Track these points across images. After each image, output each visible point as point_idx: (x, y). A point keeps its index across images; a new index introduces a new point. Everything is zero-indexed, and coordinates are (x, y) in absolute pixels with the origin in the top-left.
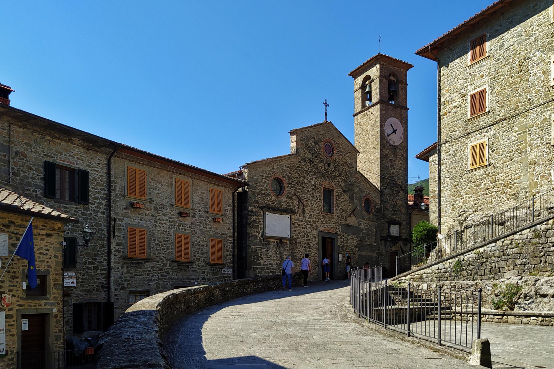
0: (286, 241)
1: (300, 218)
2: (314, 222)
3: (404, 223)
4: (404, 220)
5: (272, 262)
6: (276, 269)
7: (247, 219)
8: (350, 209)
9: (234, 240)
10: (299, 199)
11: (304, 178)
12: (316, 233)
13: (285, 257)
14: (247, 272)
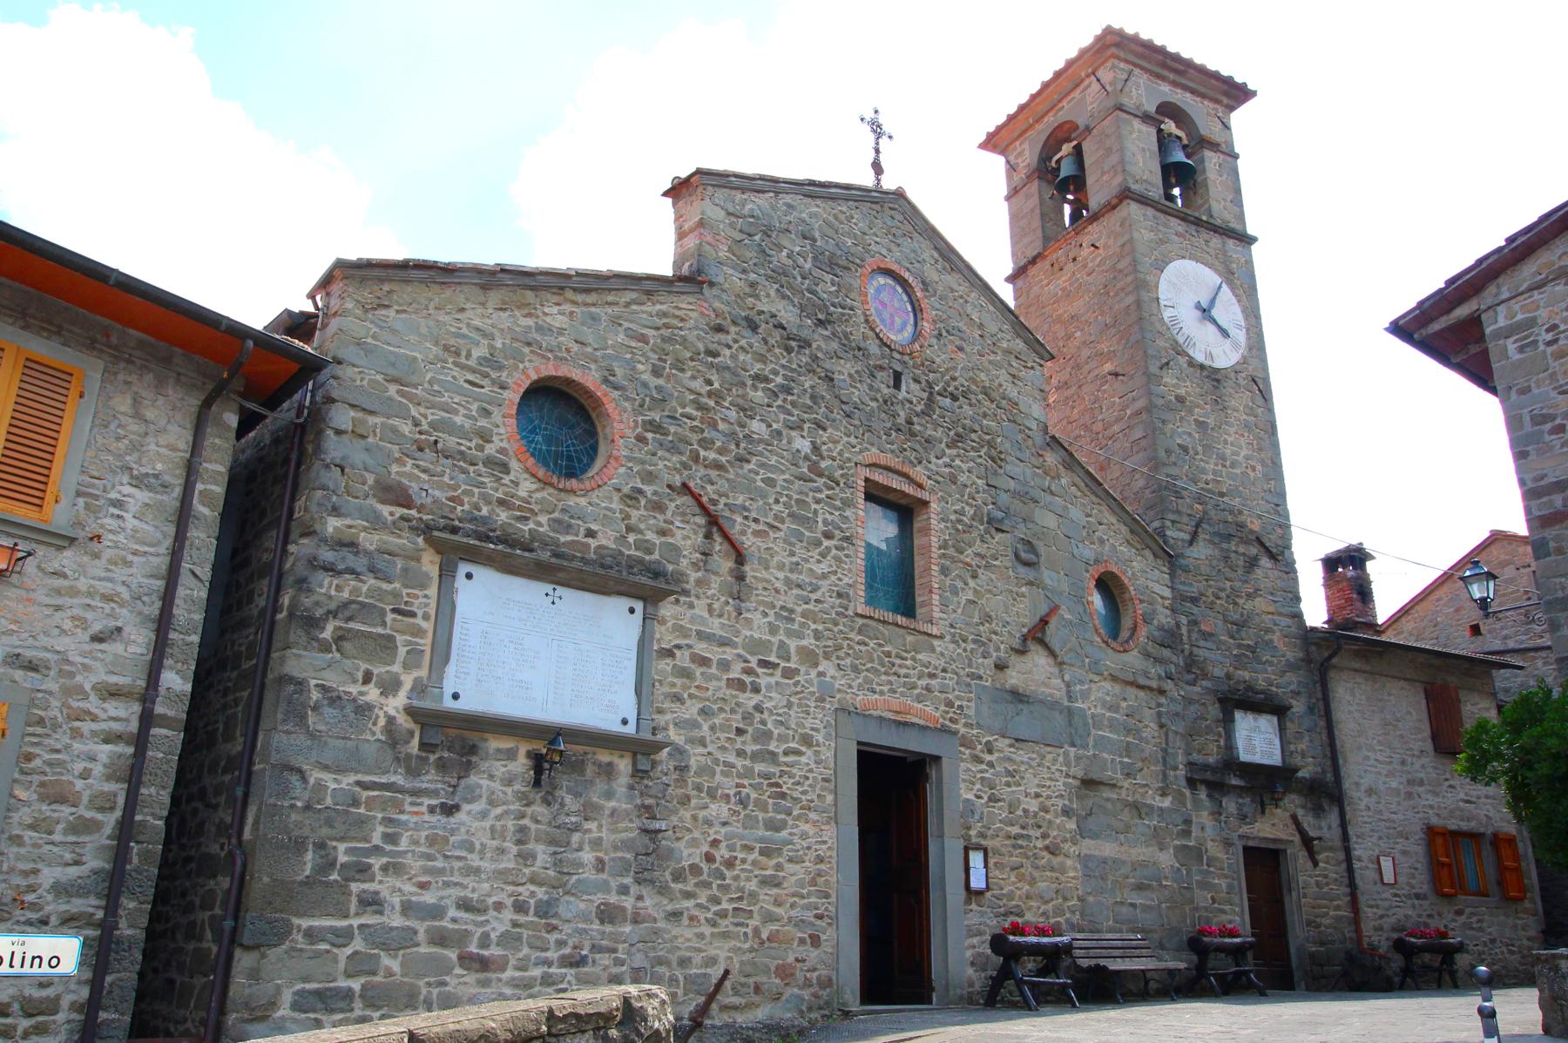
0: (604, 757)
1: (715, 626)
2: (809, 657)
3: (1298, 706)
5: (477, 889)
6: (509, 940)
7: (302, 583)
8: (1024, 613)
9: (147, 719)
10: (714, 523)
11: (747, 411)
12: (817, 721)
13: (587, 856)
14: (243, 961)
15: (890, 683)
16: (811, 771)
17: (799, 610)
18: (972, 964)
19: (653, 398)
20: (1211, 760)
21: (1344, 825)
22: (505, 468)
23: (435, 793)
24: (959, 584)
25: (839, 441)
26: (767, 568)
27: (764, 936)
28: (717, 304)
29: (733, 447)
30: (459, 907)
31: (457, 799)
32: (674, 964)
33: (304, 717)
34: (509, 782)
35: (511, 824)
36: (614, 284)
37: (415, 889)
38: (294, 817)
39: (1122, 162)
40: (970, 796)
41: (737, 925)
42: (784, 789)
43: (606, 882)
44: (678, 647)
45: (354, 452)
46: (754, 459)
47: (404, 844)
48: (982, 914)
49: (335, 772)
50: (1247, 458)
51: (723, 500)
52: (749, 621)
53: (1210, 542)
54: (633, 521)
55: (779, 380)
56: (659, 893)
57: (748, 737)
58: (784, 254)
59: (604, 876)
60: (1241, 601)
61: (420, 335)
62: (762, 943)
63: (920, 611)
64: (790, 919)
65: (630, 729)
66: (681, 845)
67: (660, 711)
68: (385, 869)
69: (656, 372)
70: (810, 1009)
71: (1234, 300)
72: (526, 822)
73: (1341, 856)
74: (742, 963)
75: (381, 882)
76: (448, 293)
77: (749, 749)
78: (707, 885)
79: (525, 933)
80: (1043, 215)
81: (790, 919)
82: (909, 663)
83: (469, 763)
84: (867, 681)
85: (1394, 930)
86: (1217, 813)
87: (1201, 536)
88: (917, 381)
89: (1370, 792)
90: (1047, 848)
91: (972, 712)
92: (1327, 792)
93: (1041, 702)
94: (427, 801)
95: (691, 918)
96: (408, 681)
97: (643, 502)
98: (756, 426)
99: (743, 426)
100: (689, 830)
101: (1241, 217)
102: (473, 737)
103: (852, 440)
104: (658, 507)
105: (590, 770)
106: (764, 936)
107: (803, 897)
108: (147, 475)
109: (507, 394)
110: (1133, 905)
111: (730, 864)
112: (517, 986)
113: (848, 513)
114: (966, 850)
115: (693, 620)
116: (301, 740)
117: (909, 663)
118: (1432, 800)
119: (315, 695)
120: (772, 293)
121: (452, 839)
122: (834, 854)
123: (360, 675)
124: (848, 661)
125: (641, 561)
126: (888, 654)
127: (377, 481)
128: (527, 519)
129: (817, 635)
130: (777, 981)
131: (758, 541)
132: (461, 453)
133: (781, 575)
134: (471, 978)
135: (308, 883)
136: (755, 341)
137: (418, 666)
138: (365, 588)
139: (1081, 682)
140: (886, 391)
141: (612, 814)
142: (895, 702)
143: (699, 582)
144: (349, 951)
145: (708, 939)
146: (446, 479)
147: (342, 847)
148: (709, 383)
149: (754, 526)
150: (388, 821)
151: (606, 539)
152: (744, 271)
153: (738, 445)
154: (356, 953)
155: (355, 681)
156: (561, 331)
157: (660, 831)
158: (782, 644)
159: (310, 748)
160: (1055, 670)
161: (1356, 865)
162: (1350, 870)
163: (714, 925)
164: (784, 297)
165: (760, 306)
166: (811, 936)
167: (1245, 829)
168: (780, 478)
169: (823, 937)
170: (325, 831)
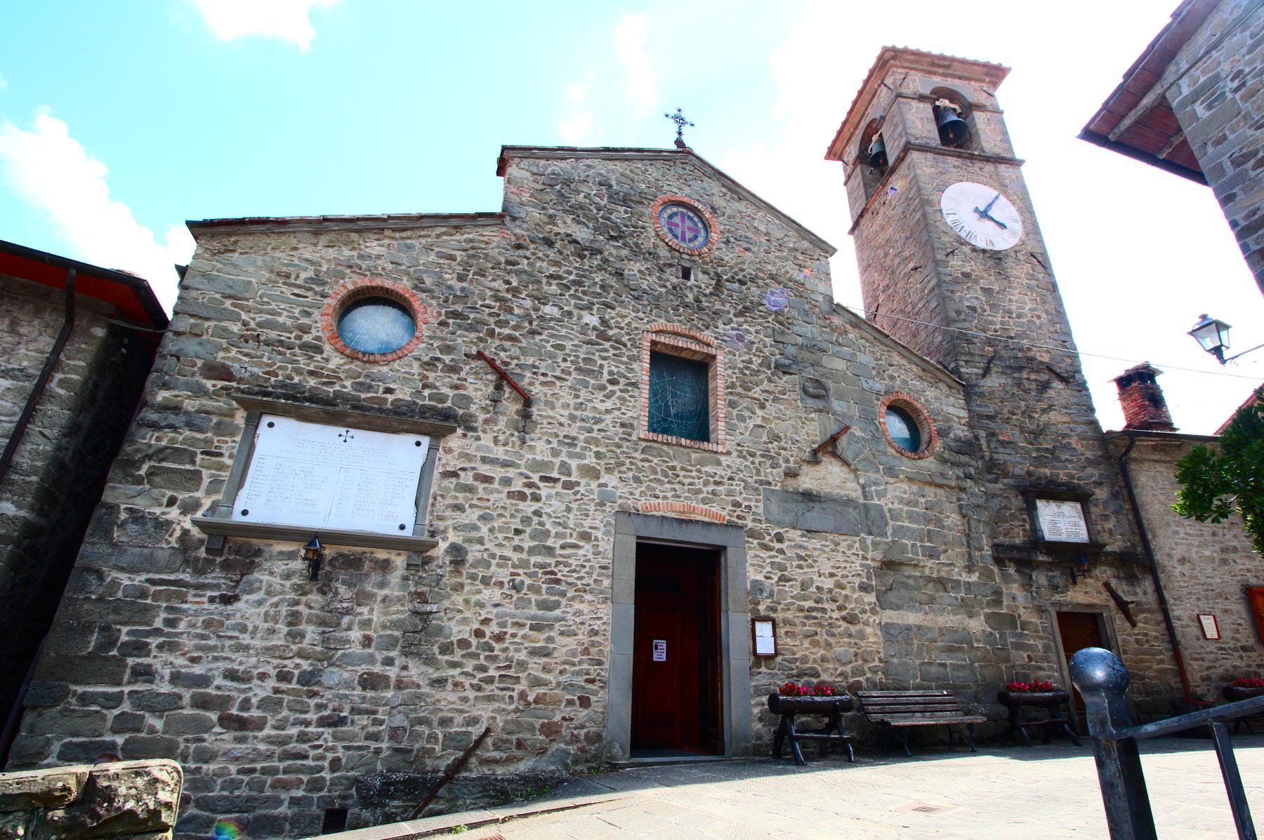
0: (381, 554)
1: (500, 453)
3: (1101, 494)
4: (1098, 484)
5: (242, 662)
6: (269, 704)
10: (503, 378)
11: (542, 299)
12: (597, 521)
13: (356, 634)
15: (675, 490)
16: (589, 561)
17: (582, 437)
18: (760, 720)
19: (455, 296)
20: (1017, 541)
21: (1158, 590)
22: (319, 350)
23: (217, 587)
24: (746, 413)
25: (626, 316)
26: (553, 408)
27: (531, 698)
28: (518, 231)
29: (526, 324)
30: (225, 677)
31: (237, 591)
32: (435, 723)
33: (111, 532)
34: (288, 576)
35: (284, 610)
36: (425, 223)
37: (187, 663)
38: (86, 607)
39: (905, 129)
40: (760, 577)
41: (502, 689)
42: (559, 576)
43: (372, 656)
44: (463, 469)
45: (190, 346)
46: (546, 332)
47: (182, 626)
48: (772, 676)
49: (129, 572)
50: (1032, 310)
51: (515, 362)
52: (532, 448)
53: (1003, 373)
54: (431, 380)
55: (572, 277)
56: (425, 663)
57: (526, 536)
58: (582, 195)
59: (370, 651)
60: (1036, 416)
61: (256, 266)
62: (529, 704)
63: (712, 436)
64: (559, 684)
65: (408, 533)
66: (452, 624)
67: (440, 518)
68: (160, 647)
69: (461, 278)
70: (575, 762)
71: (1009, 203)
72: (300, 608)
73: (1159, 617)
74: (506, 722)
75: (155, 657)
76: (284, 238)
77: (526, 545)
78: (476, 656)
79: (286, 698)
80: (865, 185)
81: (559, 684)
82: (694, 474)
83: (253, 563)
84: (648, 487)
85: (1222, 679)
86: (1028, 585)
87: (994, 370)
88: (705, 272)
89: (1182, 561)
90: (844, 619)
91: (760, 510)
92: (1139, 561)
93: (834, 500)
94: (209, 593)
95: (456, 685)
96: (207, 503)
97: (440, 366)
98: (549, 310)
99: (536, 310)
100: (460, 611)
101: (1010, 149)
102: (257, 543)
103: (641, 315)
104: (453, 369)
105: (367, 566)
106: (531, 698)
107: (574, 665)
108: (13, 369)
109: (326, 301)
110: (944, 665)
111: (499, 638)
112: (272, 743)
113: (635, 366)
114: (753, 621)
115: (478, 449)
116: (104, 549)
117: (694, 474)
118: (1248, 564)
119: (123, 516)
120: (569, 221)
121: (227, 623)
122: (609, 628)
123: (165, 500)
124: (630, 474)
125: (433, 408)
126: (673, 468)
127: (204, 365)
128: (333, 383)
129: (598, 455)
130: (542, 737)
131: (545, 389)
132: (281, 342)
133: (566, 413)
134: (229, 736)
135: (90, 657)
136: (552, 254)
137: (217, 492)
138: (181, 438)
139: (876, 484)
140: (674, 280)
141: (384, 600)
142: (678, 504)
143: (486, 421)
144: (116, 712)
145: (472, 702)
146: (265, 360)
147: (125, 629)
148: (508, 282)
149: (542, 378)
150: (170, 609)
151: (404, 394)
152: (544, 208)
153: (531, 323)
154: (123, 714)
155: (160, 505)
156: (379, 257)
157: (431, 613)
158: (563, 464)
159: (110, 555)
160: (852, 476)
161: (1176, 624)
162: (1170, 629)
163: (479, 689)
164: (579, 223)
165: (556, 230)
166: (579, 698)
167: (1057, 597)
168: (569, 345)
169: (593, 699)
170: (112, 617)
